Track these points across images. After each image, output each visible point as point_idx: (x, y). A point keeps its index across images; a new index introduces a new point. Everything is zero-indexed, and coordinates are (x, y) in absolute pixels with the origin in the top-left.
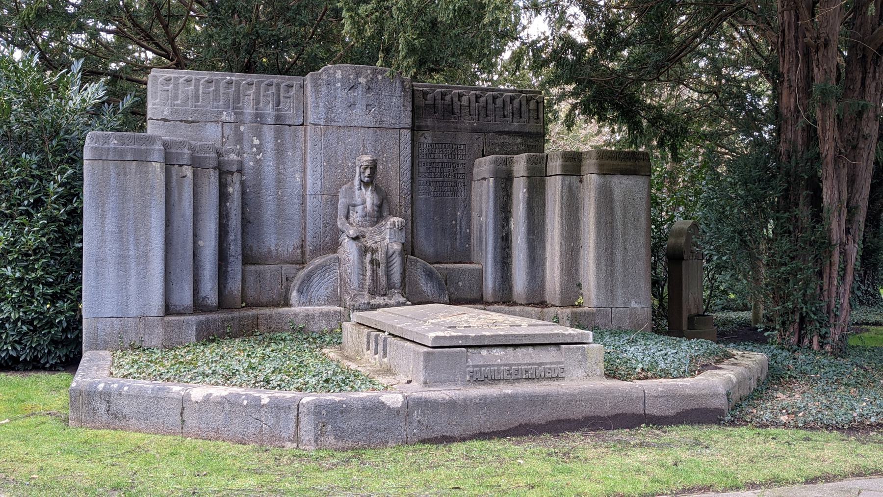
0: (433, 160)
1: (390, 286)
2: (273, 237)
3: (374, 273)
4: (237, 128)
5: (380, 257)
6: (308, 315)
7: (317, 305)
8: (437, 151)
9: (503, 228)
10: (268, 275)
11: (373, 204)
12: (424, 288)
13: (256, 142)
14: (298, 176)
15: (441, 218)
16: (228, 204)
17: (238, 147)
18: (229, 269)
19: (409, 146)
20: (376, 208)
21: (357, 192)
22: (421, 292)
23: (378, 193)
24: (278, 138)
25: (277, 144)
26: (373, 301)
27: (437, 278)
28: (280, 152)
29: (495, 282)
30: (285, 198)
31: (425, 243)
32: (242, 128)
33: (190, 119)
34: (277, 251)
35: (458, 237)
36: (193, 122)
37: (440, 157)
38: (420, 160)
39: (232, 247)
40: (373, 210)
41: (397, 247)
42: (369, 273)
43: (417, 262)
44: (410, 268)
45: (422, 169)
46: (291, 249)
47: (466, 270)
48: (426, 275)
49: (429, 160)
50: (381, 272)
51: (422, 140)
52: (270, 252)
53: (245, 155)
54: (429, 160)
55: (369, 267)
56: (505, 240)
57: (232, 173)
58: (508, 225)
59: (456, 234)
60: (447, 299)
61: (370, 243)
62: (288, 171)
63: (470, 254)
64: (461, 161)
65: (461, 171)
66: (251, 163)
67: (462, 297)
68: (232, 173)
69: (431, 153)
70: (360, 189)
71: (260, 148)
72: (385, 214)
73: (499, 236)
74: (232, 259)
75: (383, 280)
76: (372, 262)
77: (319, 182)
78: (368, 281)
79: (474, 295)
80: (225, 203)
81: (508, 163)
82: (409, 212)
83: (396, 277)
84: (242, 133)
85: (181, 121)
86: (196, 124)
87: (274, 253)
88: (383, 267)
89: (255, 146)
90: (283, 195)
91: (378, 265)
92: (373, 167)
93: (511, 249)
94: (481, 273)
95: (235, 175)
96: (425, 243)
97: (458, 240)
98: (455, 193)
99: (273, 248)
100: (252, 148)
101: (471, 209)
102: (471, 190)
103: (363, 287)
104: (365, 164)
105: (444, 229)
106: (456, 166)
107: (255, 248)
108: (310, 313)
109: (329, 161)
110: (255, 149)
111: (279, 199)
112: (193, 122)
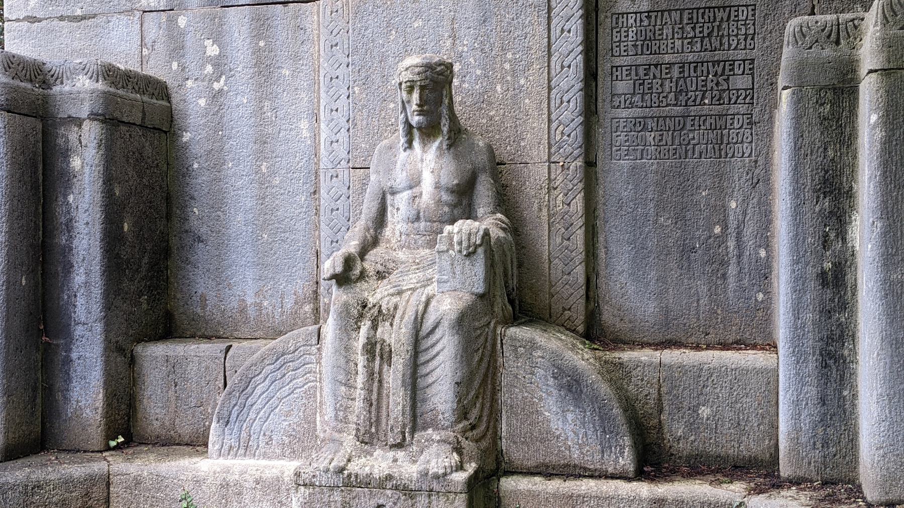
0: (653, 59)
1: (416, 419)
2: (250, 274)
3: (375, 379)
4: (172, 21)
5: (397, 335)
6: (225, 485)
7: (265, 456)
8: (667, 31)
9: (825, 243)
10: (192, 369)
11: (437, 186)
12: (556, 425)
13: (213, 50)
14: (304, 125)
15: (680, 218)
16: (71, 198)
17: (175, 65)
18: (74, 355)
19: (576, 25)
20: (446, 197)
21: (402, 155)
22: (547, 437)
23: (456, 157)
24: (258, 36)
25: (257, 51)
26: (359, 467)
27: (594, 398)
28: (264, 68)
29: (796, 417)
30: (277, 181)
31: (631, 288)
32: (182, 21)
33: (79, 12)
34: (259, 306)
35: (732, 270)
36: (83, 18)
37: (676, 50)
38: (618, 61)
39: (80, 301)
40: (439, 202)
41: (447, 306)
42: (360, 380)
43: (532, 346)
44: (511, 366)
45: (623, 86)
46: (289, 303)
47: (722, 371)
48: (560, 387)
49: (641, 60)
50: (394, 376)
52: (243, 310)
53: (189, 83)
54: (641, 60)
55: (361, 360)
56: (835, 281)
57: (78, 122)
58: (842, 235)
59: (724, 263)
60: (626, 461)
61: (378, 294)
62: (281, 114)
64: (741, 55)
65: (741, 82)
66: (202, 102)
67: (712, 450)
68: (78, 122)
69: (648, 42)
70: (410, 144)
71: (219, 63)
72: (480, 211)
73: (811, 272)
74: (79, 331)
75: (396, 400)
76: (370, 348)
77: (343, 136)
78: (358, 405)
79: (751, 446)
80: (65, 196)
81: (843, 35)
82: (578, 204)
83: (441, 393)
84: (183, 33)
85: (61, 18)
86: (89, 22)
87: (252, 312)
88: (399, 363)
89: (210, 60)
90: (273, 173)
91: (387, 357)
92: (435, 84)
93: (853, 313)
94: (771, 377)
95: (86, 125)
96: (631, 288)
97: (732, 281)
98: (721, 148)
99: (250, 300)
100: (203, 67)
103: (345, 420)
104: (407, 76)
105: (686, 251)
106: (726, 68)
107: (211, 296)
108: (231, 478)
109: (366, 82)
110: (209, 69)
111: (263, 182)
112: (83, 18)
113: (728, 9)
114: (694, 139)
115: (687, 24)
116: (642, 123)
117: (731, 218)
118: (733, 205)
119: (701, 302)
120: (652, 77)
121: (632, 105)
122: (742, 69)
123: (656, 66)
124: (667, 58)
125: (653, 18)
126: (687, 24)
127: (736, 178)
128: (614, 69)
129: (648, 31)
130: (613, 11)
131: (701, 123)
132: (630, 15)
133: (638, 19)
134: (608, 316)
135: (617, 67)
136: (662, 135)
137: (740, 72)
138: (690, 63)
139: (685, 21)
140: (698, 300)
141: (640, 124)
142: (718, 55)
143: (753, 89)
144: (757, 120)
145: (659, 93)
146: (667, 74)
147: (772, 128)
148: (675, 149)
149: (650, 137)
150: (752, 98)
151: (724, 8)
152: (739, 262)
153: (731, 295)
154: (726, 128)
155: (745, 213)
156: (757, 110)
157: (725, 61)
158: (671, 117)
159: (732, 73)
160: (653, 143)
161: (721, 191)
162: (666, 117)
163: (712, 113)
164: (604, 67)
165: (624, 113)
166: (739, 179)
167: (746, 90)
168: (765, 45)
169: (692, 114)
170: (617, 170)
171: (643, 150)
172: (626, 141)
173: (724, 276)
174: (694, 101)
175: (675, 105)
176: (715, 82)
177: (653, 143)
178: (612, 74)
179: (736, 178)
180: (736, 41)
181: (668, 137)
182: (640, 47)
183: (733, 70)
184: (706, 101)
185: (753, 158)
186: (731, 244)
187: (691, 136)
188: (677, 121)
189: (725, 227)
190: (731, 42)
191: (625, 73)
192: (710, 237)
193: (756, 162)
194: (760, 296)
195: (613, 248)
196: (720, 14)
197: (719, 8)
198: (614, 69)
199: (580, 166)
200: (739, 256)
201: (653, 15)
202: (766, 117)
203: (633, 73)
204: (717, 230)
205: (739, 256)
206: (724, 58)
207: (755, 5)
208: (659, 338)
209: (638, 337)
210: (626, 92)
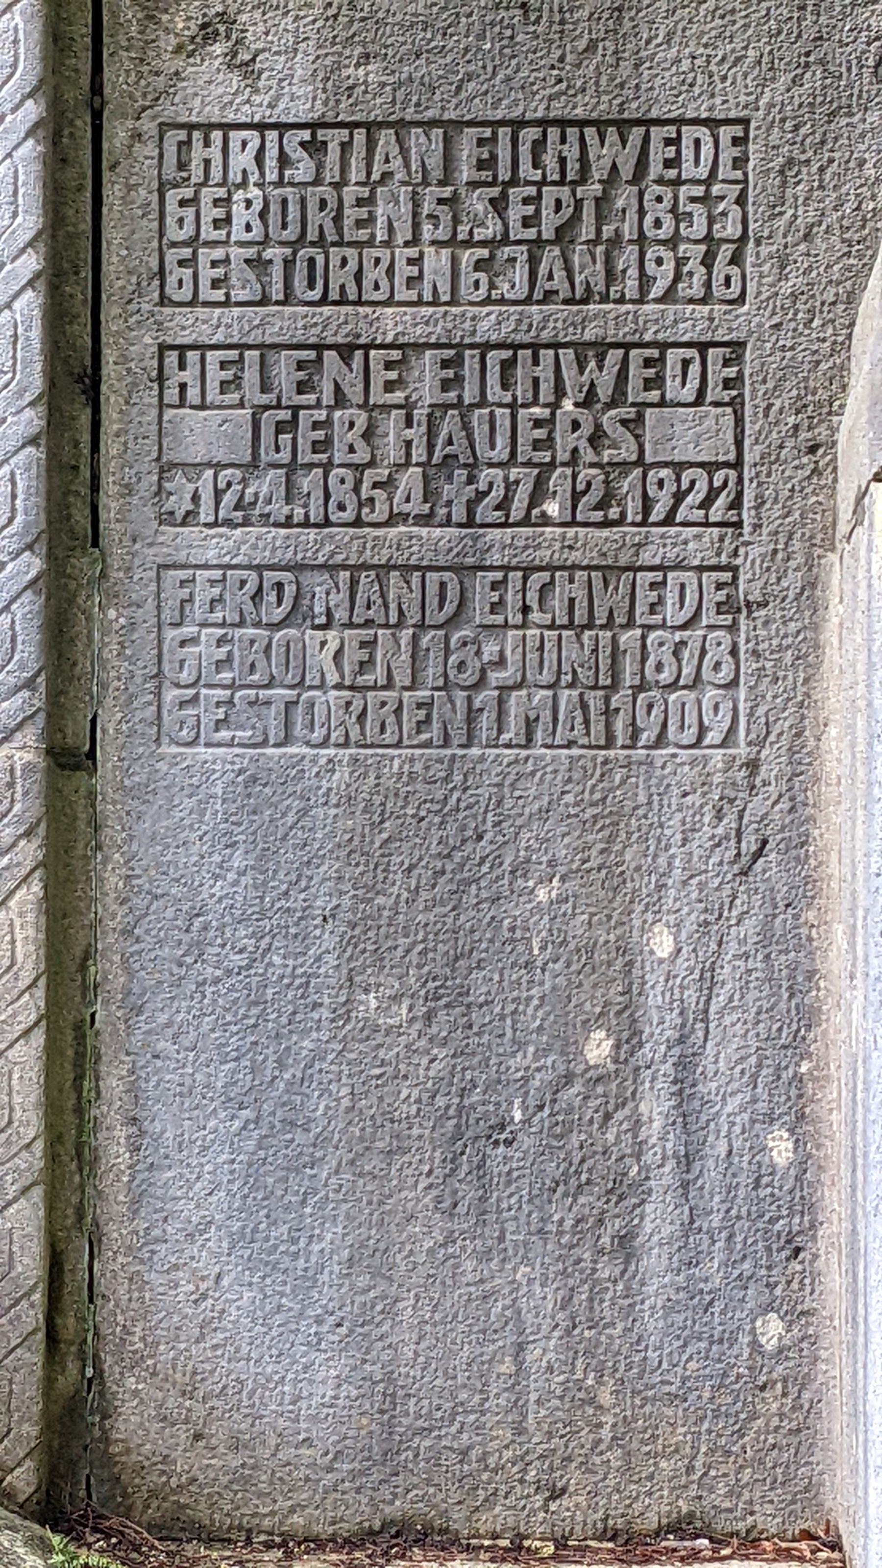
0: (336, 324)
15: (444, 996)
31: (239, 1300)
35: (658, 1219)
37: (426, 291)
38: (187, 327)
45: (208, 433)
49: (284, 323)
51: (209, 88)
54: (284, 323)
59: (625, 1191)
63: (802, 1428)
64: (691, 322)
65: (690, 434)
69: (311, 251)
96: (239, 1300)
97: (655, 1262)
98: (609, 703)
101: (805, 889)
102: (807, 654)
105: (472, 1136)
106: (631, 376)
113: (637, 132)
114: (501, 662)
115: (473, 185)
116: (289, 591)
117: (654, 998)
118: (662, 943)
119: (532, 1354)
120: (328, 398)
121: (245, 513)
122: (693, 383)
123: (346, 351)
124: (392, 323)
125: (334, 149)
126: (473, 185)
127: (673, 830)
128: (172, 358)
129: (312, 206)
130: (168, 111)
131: (532, 598)
132: (236, 136)
133: (271, 153)
134: (138, 1422)
135: (182, 349)
136: (369, 644)
137: (688, 393)
138: (486, 347)
139: (465, 173)
140: (520, 1348)
141: (280, 595)
142: (600, 321)
143: (737, 464)
144: (756, 596)
145: (359, 468)
146: (389, 386)
147: (815, 627)
148: (425, 705)
149: (321, 649)
150: (736, 504)
151: (623, 125)
152: (685, 1185)
153: (652, 1324)
154: (630, 624)
155: (708, 980)
156: (755, 551)
157: (627, 346)
158: (406, 569)
159: (654, 395)
160: (332, 678)
161: (612, 885)
162: (389, 567)
163: (575, 557)
164: (129, 348)
165: (211, 546)
166: (685, 842)
167: (710, 467)
168: (786, 288)
169: (495, 558)
170: (188, 788)
171: (290, 705)
172: (220, 665)
173: (625, 1243)
174: (503, 505)
175: (425, 520)
176: (586, 430)
177: (332, 678)
178: (161, 378)
179: (673, 830)
180: (669, 267)
181: (393, 653)
182: (277, 272)
183: (655, 382)
184: (552, 508)
185: (742, 751)
186: (655, 1107)
187: (490, 650)
188: (432, 590)
189: (629, 1040)
190: (651, 268)
191: (215, 376)
192: (568, 1078)
193: (753, 765)
194: (772, 1331)
195: (164, 1124)
196: (605, 153)
197: (600, 125)
198: (172, 358)
199: (28, 768)
200: (687, 1161)
201: (334, 138)
202: (793, 581)
203: (251, 376)
204: (598, 1048)
205: (687, 1161)
206: (623, 333)
207: (745, 122)
208: (358, 1513)
209: (267, 1511)
210: (220, 456)
